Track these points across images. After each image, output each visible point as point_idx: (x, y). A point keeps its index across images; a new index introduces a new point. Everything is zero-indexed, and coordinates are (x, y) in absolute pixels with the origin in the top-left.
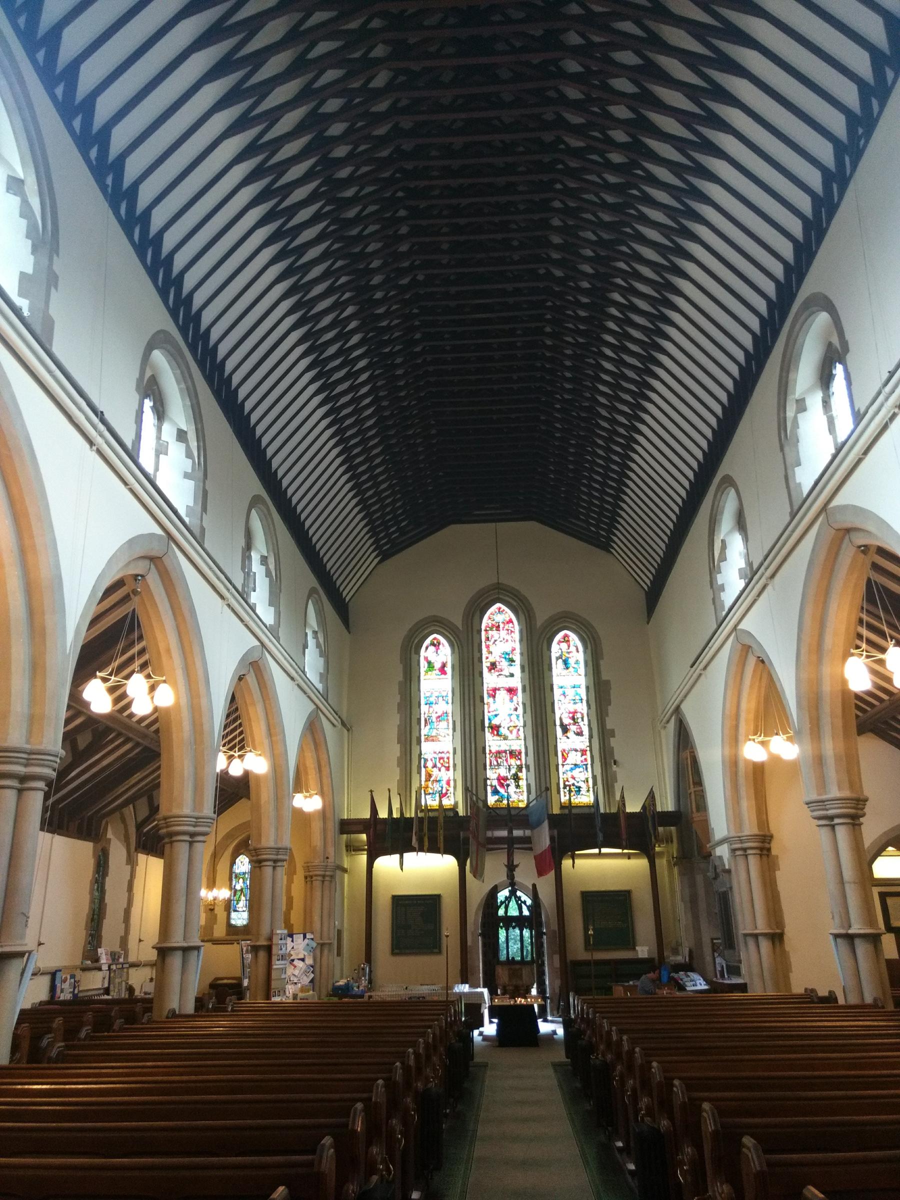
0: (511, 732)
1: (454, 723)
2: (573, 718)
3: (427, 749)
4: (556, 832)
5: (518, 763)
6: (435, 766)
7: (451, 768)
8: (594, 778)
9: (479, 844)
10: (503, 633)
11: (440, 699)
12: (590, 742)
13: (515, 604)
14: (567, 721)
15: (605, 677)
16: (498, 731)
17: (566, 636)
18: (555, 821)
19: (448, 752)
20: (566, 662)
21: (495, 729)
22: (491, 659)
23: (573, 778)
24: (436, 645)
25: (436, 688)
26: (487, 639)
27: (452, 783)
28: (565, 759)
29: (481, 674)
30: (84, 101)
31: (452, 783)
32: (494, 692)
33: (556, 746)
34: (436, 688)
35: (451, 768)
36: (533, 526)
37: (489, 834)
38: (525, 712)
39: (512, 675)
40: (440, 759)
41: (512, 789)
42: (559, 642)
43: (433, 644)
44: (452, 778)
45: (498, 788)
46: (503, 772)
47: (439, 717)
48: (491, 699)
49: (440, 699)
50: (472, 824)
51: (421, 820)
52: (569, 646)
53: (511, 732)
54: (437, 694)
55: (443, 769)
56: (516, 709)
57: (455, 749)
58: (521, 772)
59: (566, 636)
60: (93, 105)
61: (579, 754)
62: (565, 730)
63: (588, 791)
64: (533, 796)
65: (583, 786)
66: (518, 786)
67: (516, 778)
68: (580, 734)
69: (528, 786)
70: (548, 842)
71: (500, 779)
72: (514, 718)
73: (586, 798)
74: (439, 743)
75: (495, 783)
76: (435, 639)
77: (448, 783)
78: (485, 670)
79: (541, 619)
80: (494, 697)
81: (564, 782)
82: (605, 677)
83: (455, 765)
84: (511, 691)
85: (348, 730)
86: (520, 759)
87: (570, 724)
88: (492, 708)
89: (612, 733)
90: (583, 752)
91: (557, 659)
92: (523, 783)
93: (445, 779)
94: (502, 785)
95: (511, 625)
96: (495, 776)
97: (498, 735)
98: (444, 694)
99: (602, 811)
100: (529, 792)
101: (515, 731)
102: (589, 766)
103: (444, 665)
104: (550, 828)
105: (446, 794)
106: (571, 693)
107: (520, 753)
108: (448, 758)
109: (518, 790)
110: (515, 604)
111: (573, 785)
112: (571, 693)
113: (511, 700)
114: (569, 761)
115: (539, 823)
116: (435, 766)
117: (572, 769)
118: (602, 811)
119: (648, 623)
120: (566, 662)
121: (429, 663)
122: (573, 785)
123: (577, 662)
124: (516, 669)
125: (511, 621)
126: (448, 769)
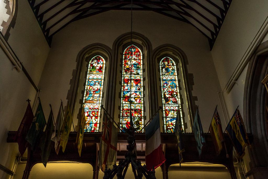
0: (136, 100)
2: (171, 95)
3: (87, 106)
5: (140, 116)
10: (134, 57)
11: (97, 83)
12: (182, 106)
14: (167, 96)
15: (189, 72)
19: (98, 109)
20: (167, 70)
21: (128, 99)
22: (127, 67)
25: (96, 78)
26: (126, 58)
27: (98, 125)
28: (167, 115)
29: (121, 72)
30: (44, 22)
31: (98, 125)
32: (127, 81)
34: (96, 78)
35: (99, 118)
38: (144, 89)
39: (138, 74)
40: (93, 112)
42: (163, 61)
43: (96, 59)
44: (98, 122)
47: (94, 92)
48: (126, 85)
49: (97, 83)
52: (169, 63)
53: (136, 100)
54: (95, 80)
55: (94, 118)
56: (139, 89)
58: (141, 120)
59: (166, 59)
60: (46, 23)
62: (167, 100)
68: (176, 102)
72: (138, 93)
76: (98, 57)
77: (96, 124)
78: (123, 71)
79: (154, 47)
81: (167, 127)
82: (189, 72)
84: (137, 81)
85: (37, 91)
86: (141, 114)
87: (170, 97)
88: (126, 88)
89: (196, 98)
91: (162, 68)
93: (94, 122)
95: (138, 53)
98: (100, 81)
101: (138, 100)
106: (170, 83)
107: (141, 110)
108: (98, 112)
112: (170, 83)
113: (137, 85)
114: (169, 115)
117: (171, 120)
119: (211, 50)
120: (167, 70)
121: (93, 67)
123: (173, 70)
124: (140, 72)
125: (139, 52)
126: (96, 117)
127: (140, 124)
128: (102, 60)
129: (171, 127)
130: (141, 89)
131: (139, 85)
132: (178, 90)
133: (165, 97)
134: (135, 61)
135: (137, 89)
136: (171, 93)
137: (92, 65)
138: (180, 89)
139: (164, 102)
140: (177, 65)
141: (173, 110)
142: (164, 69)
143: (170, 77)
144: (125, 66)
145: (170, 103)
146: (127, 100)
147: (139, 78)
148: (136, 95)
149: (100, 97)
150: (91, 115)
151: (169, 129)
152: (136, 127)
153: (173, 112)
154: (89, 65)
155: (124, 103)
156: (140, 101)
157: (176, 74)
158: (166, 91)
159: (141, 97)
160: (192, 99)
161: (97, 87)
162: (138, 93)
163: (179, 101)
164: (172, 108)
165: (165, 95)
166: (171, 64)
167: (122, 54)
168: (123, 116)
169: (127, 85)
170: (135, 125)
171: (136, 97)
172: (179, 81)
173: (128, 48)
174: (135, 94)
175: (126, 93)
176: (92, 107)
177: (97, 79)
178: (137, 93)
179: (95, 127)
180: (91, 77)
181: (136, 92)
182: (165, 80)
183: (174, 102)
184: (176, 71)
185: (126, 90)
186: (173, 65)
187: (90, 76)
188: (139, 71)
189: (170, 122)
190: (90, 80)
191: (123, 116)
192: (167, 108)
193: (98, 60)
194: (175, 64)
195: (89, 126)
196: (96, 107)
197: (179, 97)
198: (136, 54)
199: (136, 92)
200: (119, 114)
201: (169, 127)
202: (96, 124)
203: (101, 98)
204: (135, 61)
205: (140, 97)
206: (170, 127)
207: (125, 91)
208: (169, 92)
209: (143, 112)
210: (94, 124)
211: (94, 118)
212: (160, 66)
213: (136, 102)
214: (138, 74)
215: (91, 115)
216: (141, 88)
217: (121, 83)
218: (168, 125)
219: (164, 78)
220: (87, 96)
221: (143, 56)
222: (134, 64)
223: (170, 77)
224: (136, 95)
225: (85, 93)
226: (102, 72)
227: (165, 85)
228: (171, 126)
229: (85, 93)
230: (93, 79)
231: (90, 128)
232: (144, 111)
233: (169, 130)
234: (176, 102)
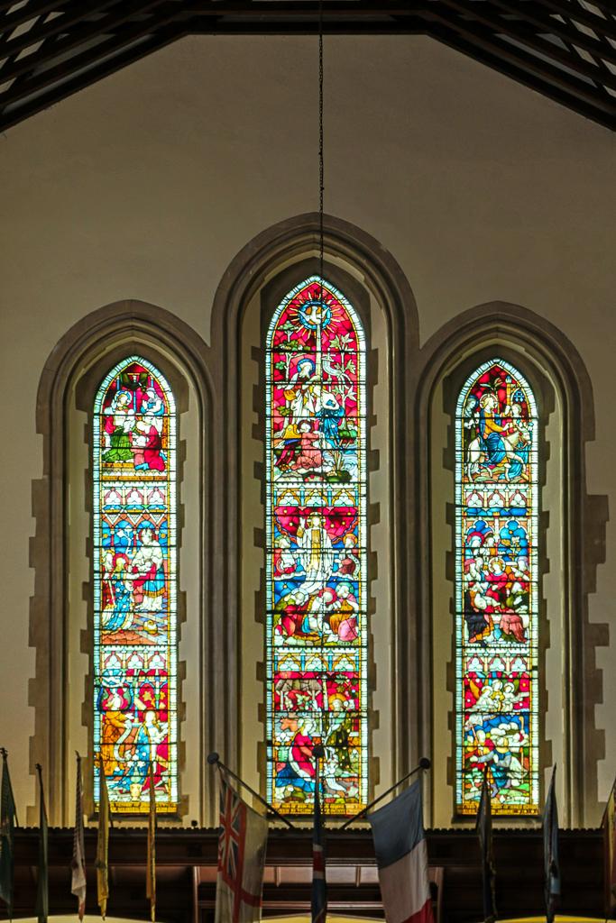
0: (335, 628)
1: (182, 597)
2: (501, 596)
3: (112, 662)
4: (439, 871)
5: (351, 704)
6: (127, 708)
7: (173, 716)
8: (545, 747)
9: (241, 896)
12: (542, 657)
13: (360, 276)
14: (481, 602)
16: (299, 624)
17: (495, 373)
18: (441, 846)
19: (164, 673)
20: (489, 447)
22: (289, 432)
23: (490, 745)
24: (136, 385)
25: (140, 503)
26: (280, 375)
27: (173, 751)
28: (471, 699)
29: (260, 470)
31: (173, 751)
33: (451, 666)
34: (140, 503)
35: (173, 716)
36: (419, 52)
37: (269, 874)
38: (373, 574)
40: (143, 689)
41: (330, 769)
42: (477, 391)
43: (129, 386)
44: (173, 738)
45: (295, 766)
46: (308, 727)
47: (137, 583)
50: (226, 846)
51: (91, 837)
53: (335, 628)
54: (135, 520)
55: (150, 716)
56: (350, 568)
57: (182, 666)
58: (357, 727)
59: (495, 373)
61: (510, 687)
62: (478, 623)
63: (528, 779)
64: (386, 782)
65: (515, 765)
66: (345, 764)
67: (343, 742)
68: (517, 636)
69: (374, 762)
70: (424, 895)
71: (298, 742)
72: (343, 590)
73: (519, 798)
74: (145, 647)
75: (286, 754)
80: (293, 532)
81: (467, 756)
83: (181, 706)
84: (339, 519)
86: (356, 698)
87: (490, 610)
88: (288, 560)
90: (522, 682)
92: (361, 756)
93: (157, 738)
94: (304, 761)
95: (346, 339)
96: (286, 737)
97: (299, 632)
98: (157, 520)
99: (562, 825)
100: (374, 780)
101: (344, 628)
102: (535, 720)
103: (156, 442)
104: (432, 862)
105: (158, 777)
106: (499, 530)
107: (354, 678)
108: (165, 688)
109: (346, 774)
110: (360, 276)
111: (491, 762)
113: (338, 544)
114: (484, 702)
115: (400, 851)
116: (127, 708)
117: (488, 726)
118: (562, 825)
120: (489, 447)
121: (117, 434)
122: (491, 762)
123: (522, 447)
124: (355, 464)
125: (348, 328)
126: (163, 715)
127: (354, 747)
128: (159, 391)
129: (483, 759)
130: (357, 569)
131: (348, 542)
132: (535, 569)
133: (470, 610)
134: (327, 389)
135: (340, 566)
136: (500, 587)
137: (108, 421)
138: (544, 567)
139: (463, 633)
140: (543, 422)
141: (500, 676)
142: (475, 445)
143: (504, 495)
144: (277, 428)
145: (489, 639)
146: (293, 626)
147: (350, 503)
148: (336, 598)
149: (165, 611)
150: (140, 706)
151: (475, 764)
152: (335, 756)
153: (498, 684)
154: (97, 422)
155: (279, 640)
156: (352, 629)
157: (535, 477)
158: (474, 576)
159: (357, 608)
160: (583, 637)
161: (148, 555)
162: (343, 590)
163: (531, 623)
164: (497, 666)
165: (468, 597)
166: (516, 410)
167: (259, 354)
168: (276, 709)
169: (293, 548)
170: (330, 749)
171: (333, 612)
172: (544, 518)
173: (293, 303)
174: (328, 596)
175: (287, 591)
176: (135, 664)
177: (145, 512)
178: (338, 587)
179: (161, 759)
180: (113, 500)
181: (332, 582)
182: (476, 512)
183: (510, 637)
184: (535, 457)
185: (288, 571)
186: (525, 416)
187: (107, 496)
188: (349, 458)
189: (482, 735)
190: (113, 520)
191: (276, 709)
192: (475, 666)
193: (136, 385)
194: (534, 412)
195: (136, 758)
196: (156, 664)
197: (535, 609)
198: (334, 344)
199: (333, 585)
200: (262, 702)
201: (474, 759)
202: (163, 749)
203: (173, 619)
204: (327, 389)
205: (352, 612)
206: (478, 756)
207: (284, 577)
208: (493, 580)
209: (364, 687)
210: (154, 748)
211: (150, 716)
212: (458, 424)
213: (332, 638)
214: (345, 477)
215: (140, 706)
216: (360, 560)
217: (260, 537)
218: (470, 749)
219: (474, 502)
220: (110, 608)
221: (372, 355)
222: (327, 414)
223: (504, 495)
224: (336, 598)
225: (97, 593)
226: (161, 466)
227: (476, 541)
228: (486, 750)
229: (97, 593)
230: (124, 511)
231: (141, 764)
232: (372, 685)
233: (476, 769)
234: (517, 636)
